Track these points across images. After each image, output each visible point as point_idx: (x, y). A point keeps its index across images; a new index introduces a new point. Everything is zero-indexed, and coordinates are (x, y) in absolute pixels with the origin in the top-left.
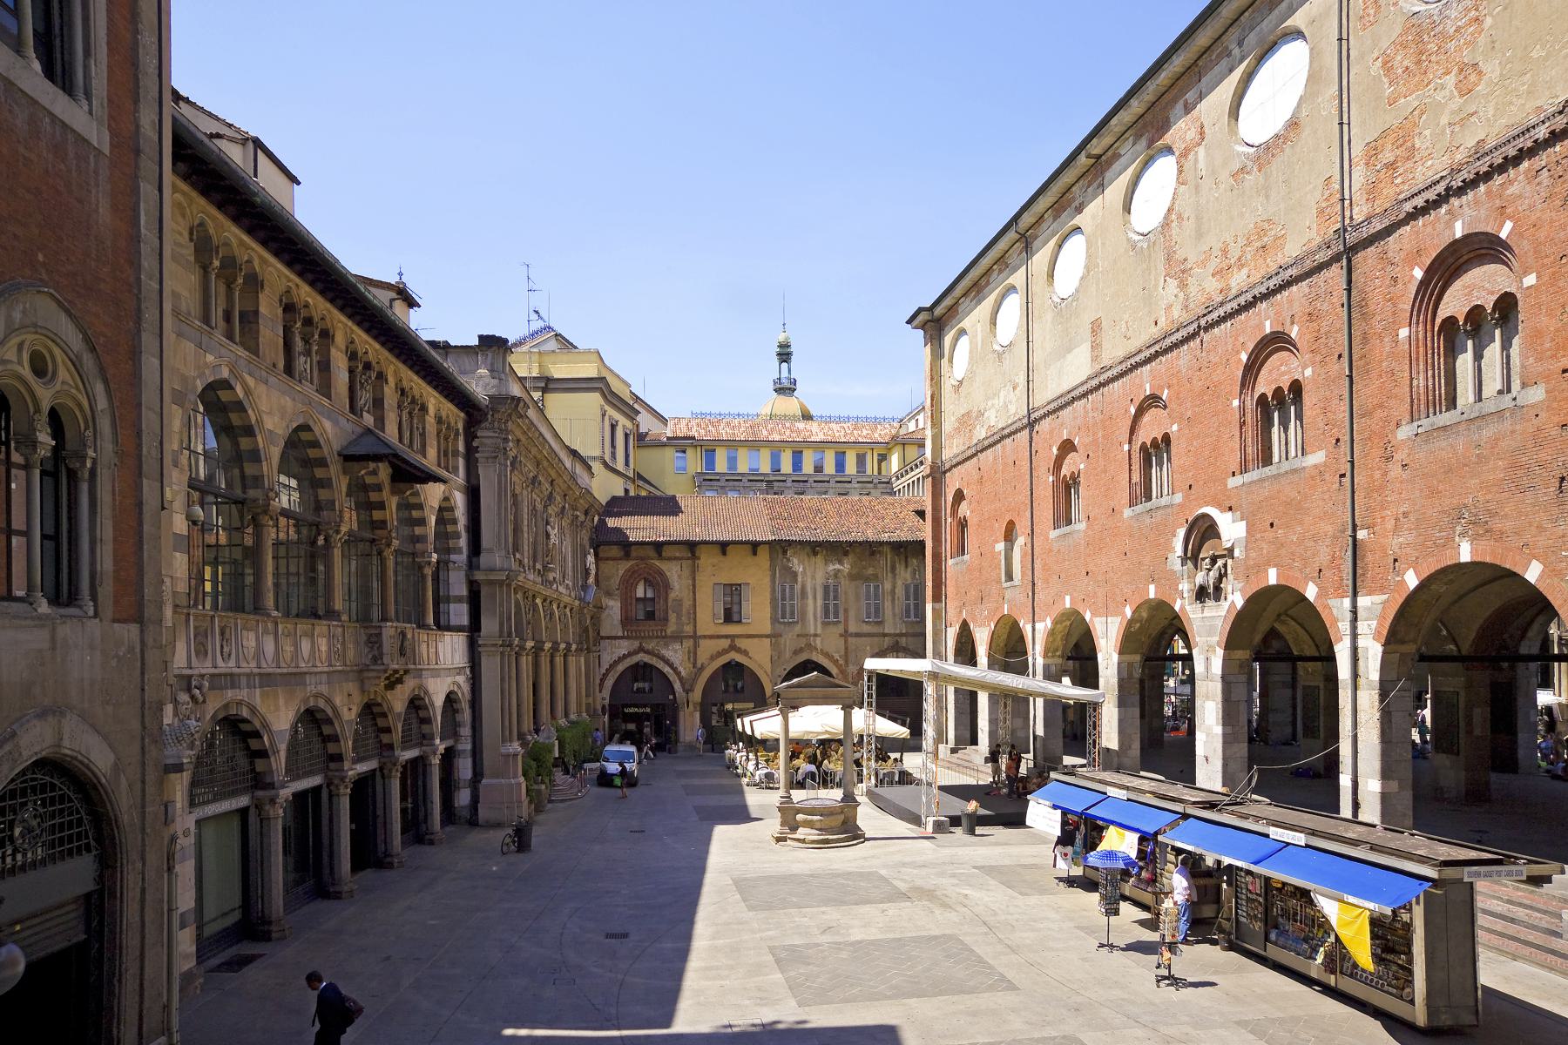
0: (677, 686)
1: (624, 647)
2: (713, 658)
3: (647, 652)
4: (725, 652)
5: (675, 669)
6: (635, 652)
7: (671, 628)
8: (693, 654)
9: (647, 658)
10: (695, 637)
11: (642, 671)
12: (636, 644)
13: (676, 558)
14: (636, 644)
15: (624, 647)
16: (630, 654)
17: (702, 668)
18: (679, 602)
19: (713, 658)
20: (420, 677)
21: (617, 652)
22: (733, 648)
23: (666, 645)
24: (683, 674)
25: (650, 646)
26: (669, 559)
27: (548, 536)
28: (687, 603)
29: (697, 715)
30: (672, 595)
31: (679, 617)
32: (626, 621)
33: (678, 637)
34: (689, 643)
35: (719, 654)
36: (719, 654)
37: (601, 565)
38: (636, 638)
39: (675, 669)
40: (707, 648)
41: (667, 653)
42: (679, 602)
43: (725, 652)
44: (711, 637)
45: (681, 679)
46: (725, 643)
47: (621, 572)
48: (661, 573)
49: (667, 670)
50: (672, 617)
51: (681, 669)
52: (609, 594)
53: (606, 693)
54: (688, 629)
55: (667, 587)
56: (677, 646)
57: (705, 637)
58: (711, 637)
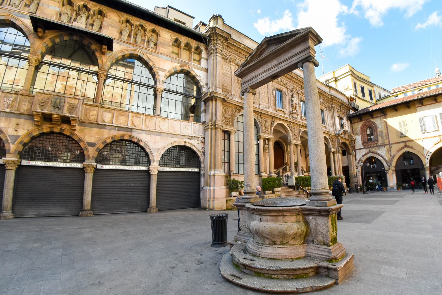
0: (385, 164)
1: (364, 152)
2: (398, 151)
3: (372, 153)
4: (403, 148)
5: (383, 158)
6: (368, 153)
7: (380, 142)
8: (390, 151)
9: (372, 155)
10: (389, 144)
11: (370, 160)
12: (367, 150)
13: (378, 117)
14: (367, 150)
15: (364, 152)
16: (366, 154)
17: (394, 156)
18: (382, 132)
19: (398, 151)
20: (131, 132)
21: (361, 154)
22: (406, 146)
23: (379, 149)
24: (387, 159)
25: (373, 150)
26: (376, 117)
27: (292, 101)
28: (385, 132)
29: (394, 175)
30: (379, 130)
31: (382, 138)
32: (363, 143)
33: (383, 145)
34: (387, 147)
35: (401, 149)
36: (401, 149)
37: (354, 125)
38: (368, 148)
39: (383, 158)
40: (395, 148)
41: (379, 152)
42: (382, 132)
43: (403, 148)
44: (396, 143)
45: (386, 161)
46: (402, 145)
47: (360, 126)
48: (374, 123)
49: (380, 158)
50: (380, 138)
51: (385, 157)
52: (357, 134)
53: (359, 169)
54: (387, 142)
55: (377, 128)
56: (383, 149)
57: (394, 143)
58: (396, 143)
